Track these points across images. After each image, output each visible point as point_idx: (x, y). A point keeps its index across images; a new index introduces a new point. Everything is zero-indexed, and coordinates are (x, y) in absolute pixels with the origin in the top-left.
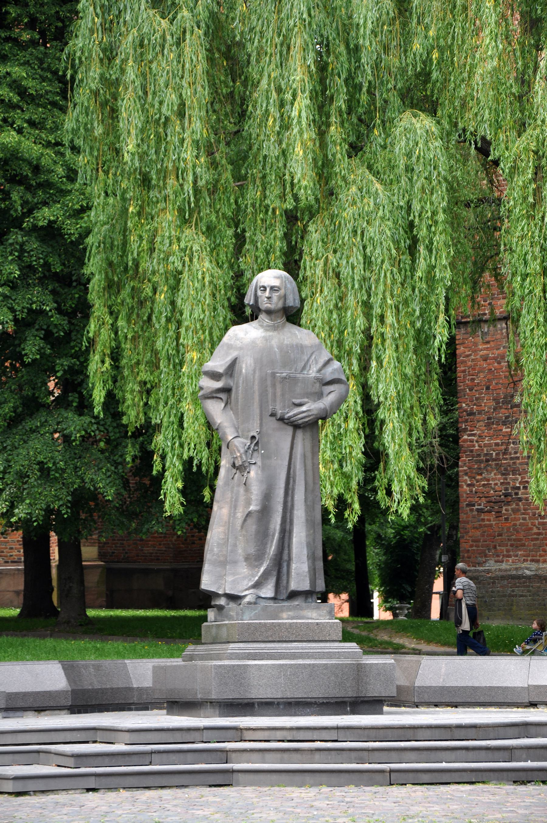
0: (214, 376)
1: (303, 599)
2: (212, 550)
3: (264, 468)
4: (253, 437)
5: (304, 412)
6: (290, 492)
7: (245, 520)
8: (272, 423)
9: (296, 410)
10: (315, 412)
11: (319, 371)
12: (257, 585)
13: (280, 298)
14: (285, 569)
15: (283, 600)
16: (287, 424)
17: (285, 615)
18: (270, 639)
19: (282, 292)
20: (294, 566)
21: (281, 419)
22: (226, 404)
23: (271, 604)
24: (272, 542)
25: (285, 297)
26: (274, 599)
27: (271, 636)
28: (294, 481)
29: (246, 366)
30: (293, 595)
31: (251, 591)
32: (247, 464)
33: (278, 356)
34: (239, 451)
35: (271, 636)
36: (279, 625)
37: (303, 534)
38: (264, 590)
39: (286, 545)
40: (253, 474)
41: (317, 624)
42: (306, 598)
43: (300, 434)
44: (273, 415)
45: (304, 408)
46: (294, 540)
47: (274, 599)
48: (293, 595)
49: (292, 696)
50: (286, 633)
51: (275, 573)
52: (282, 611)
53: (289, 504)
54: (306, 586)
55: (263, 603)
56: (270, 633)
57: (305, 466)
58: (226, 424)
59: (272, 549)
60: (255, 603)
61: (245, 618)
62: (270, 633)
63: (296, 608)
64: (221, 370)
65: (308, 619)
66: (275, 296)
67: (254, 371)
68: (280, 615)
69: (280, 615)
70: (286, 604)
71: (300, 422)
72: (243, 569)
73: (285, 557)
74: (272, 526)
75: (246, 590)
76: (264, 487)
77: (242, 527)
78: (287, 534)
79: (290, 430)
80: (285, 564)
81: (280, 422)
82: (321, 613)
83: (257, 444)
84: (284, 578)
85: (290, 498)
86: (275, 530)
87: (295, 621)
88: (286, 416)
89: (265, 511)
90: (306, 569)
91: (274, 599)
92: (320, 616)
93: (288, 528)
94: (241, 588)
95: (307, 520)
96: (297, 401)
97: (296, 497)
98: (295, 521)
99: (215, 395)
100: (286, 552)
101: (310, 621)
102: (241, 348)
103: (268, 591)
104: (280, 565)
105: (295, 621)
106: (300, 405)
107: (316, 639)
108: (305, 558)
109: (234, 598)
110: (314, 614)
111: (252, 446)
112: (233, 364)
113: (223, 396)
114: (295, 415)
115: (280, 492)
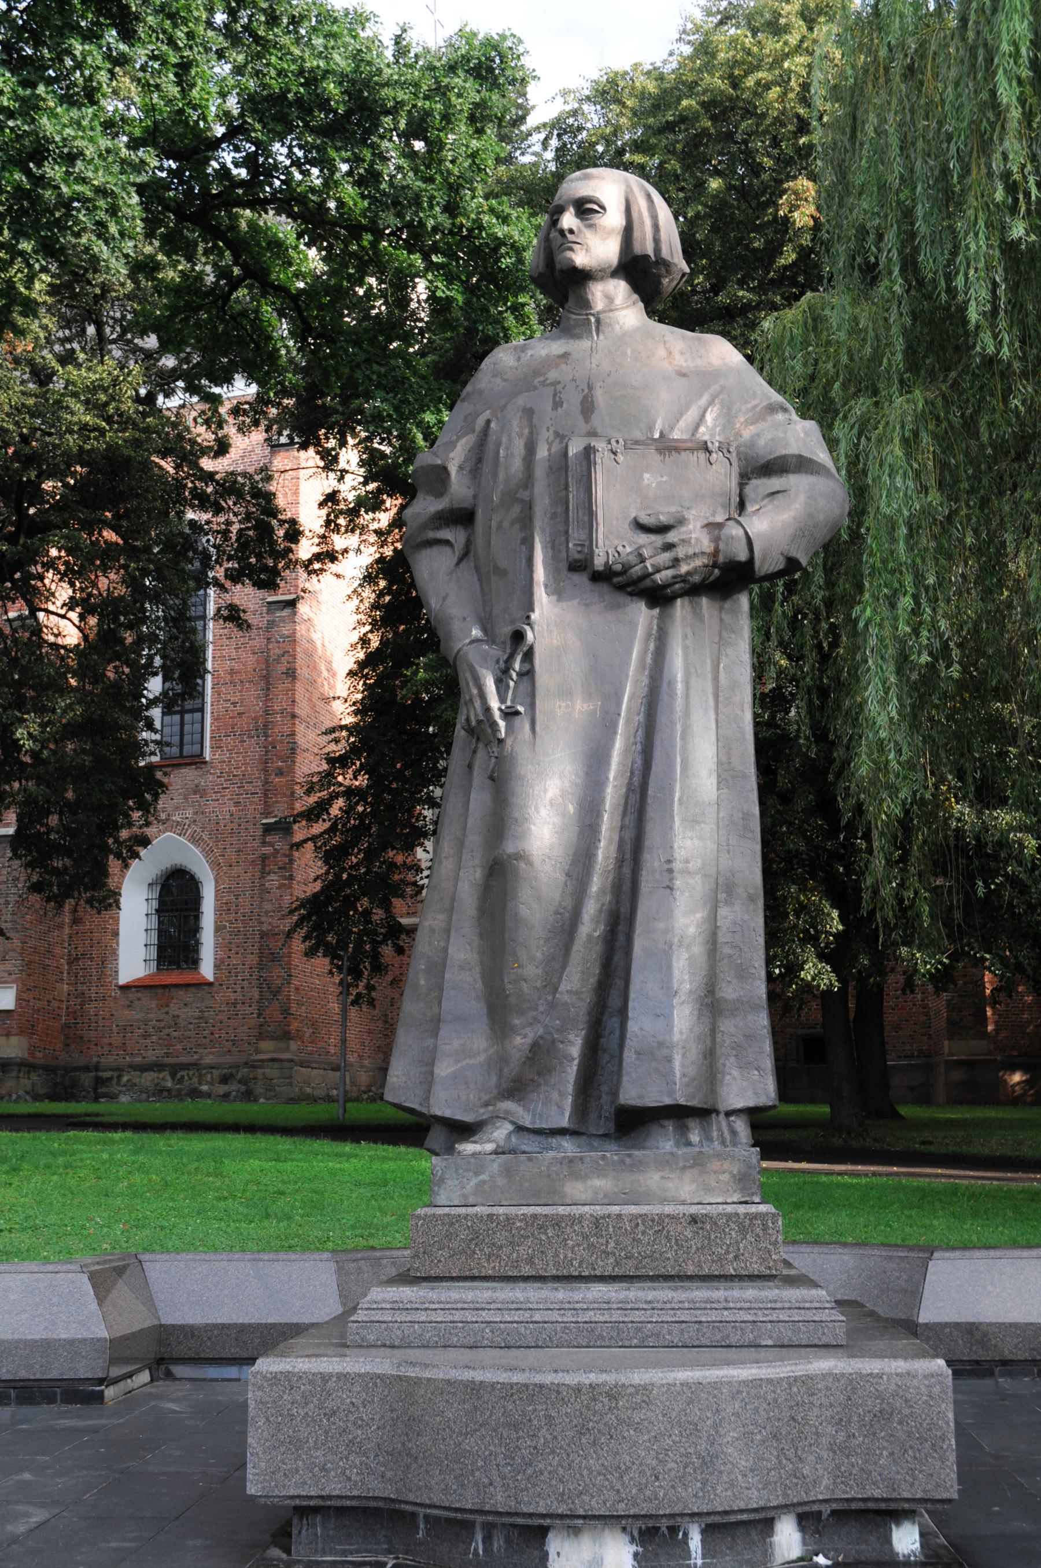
16: (621, 588)
18: (526, 1270)
20: (632, 1027)
27: (530, 1261)
35: (530, 1261)
36: (557, 1222)
41: (694, 1220)
45: (672, 537)
48: (632, 1124)
49: (512, 1505)
50: (581, 1252)
56: (523, 1251)
61: (442, 1199)
62: (523, 1251)
65: (663, 1201)
75: (487, 1104)
81: (604, 587)
87: (615, 1209)
92: (708, 1190)
99: (431, 535)
100: (619, 983)
101: (668, 1209)
105: (615, 1209)
107: (691, 1270)
113: (455, 535)
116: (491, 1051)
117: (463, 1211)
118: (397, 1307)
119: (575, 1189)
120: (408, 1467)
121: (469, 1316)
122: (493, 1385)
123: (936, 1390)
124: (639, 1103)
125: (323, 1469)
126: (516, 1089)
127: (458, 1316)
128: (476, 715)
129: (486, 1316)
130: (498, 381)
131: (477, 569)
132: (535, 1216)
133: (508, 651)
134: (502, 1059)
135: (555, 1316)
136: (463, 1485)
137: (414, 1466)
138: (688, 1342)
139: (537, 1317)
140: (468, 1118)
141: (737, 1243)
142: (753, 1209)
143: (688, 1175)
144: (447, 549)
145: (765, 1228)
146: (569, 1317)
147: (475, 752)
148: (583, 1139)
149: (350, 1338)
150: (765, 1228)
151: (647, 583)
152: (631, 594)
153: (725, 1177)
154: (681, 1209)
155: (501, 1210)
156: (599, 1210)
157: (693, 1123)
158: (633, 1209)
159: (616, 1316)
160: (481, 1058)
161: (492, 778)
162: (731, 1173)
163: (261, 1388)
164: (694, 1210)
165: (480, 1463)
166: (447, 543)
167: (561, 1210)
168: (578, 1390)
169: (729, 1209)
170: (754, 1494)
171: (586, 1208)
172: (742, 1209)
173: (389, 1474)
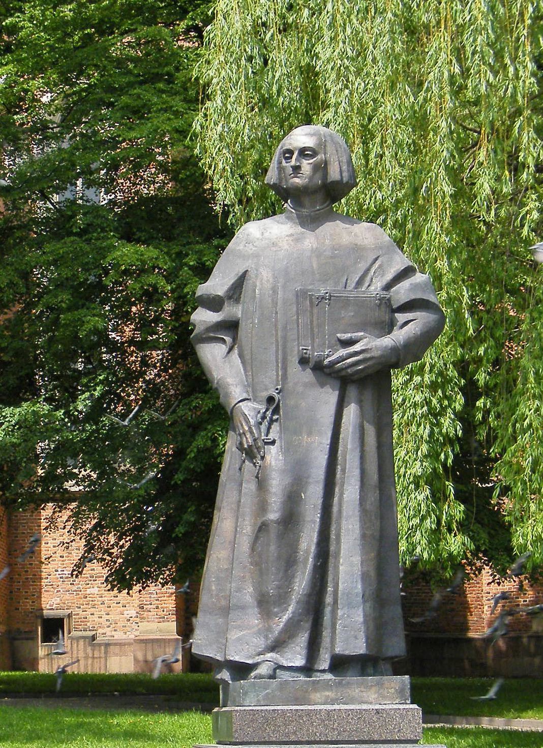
0: (215, 304)
2: (210, 590)
3: (287, 450)
4: (270, 400)
5: (356, 354)
7: (257, 538)
8: (302, 377)
9: (343, 352)
10: (376, 353)
11: (388, 287)
13: (316, 168)
14: (327, 618)
16: (329, 375)
18: (293, 738)
22: (231, 350)
24: (304, 573)
26: (308, 669)
27: (295, 733)
29: (263, 280)
30: (340, 664)
31: (269, 656)
34: (248, 422)
35: (295, 733)
37: (357, 560)
39: (330, 578)
41: (378, 712)
45: (357, 347)
50: (321, 728)
51: (307, 625)
52: (315, 690)
54: (359, 647)
55: (285, 676)
58: (230, 380)
59: (301, 584)
60: (273, 677)
61: (247, 702)
62: (291, 728)
64: (221, 292)
66: (306, 166)
67: (274, 290)
72: (254, 619)
73: (329, 599)
75: (259, 654)
76: (288, 480)
77: (253, 549)
80: (328, 610)
83: (276, 411)
84: (326, 634)
87: (336, 707)
89: (291, 519)
92: (384, 697)
101: (365, 707)
102: (256, 256)
105: (336, 707)
106: (350, 343)
107: (376, 737)
109: (242, 670)
110: (372, 695)
111: (269, 413)
112: (242, 280)
116: (261, 626)
119: (317, 696)
124: (347, 653)
126: (276, 646)
128: (247, 442)
130: (251, 246)
141: (399, 724)
142: (407, 706)
151: (343, 373)
154: (371, 707)
156: (329, 707)
160: (256, 629)
161: (257, 477)
162: (395, 688)
164: (378, 707)
167: (310, 707)
169: (395, 707)
171: (322, 707)
172: (401, 707)
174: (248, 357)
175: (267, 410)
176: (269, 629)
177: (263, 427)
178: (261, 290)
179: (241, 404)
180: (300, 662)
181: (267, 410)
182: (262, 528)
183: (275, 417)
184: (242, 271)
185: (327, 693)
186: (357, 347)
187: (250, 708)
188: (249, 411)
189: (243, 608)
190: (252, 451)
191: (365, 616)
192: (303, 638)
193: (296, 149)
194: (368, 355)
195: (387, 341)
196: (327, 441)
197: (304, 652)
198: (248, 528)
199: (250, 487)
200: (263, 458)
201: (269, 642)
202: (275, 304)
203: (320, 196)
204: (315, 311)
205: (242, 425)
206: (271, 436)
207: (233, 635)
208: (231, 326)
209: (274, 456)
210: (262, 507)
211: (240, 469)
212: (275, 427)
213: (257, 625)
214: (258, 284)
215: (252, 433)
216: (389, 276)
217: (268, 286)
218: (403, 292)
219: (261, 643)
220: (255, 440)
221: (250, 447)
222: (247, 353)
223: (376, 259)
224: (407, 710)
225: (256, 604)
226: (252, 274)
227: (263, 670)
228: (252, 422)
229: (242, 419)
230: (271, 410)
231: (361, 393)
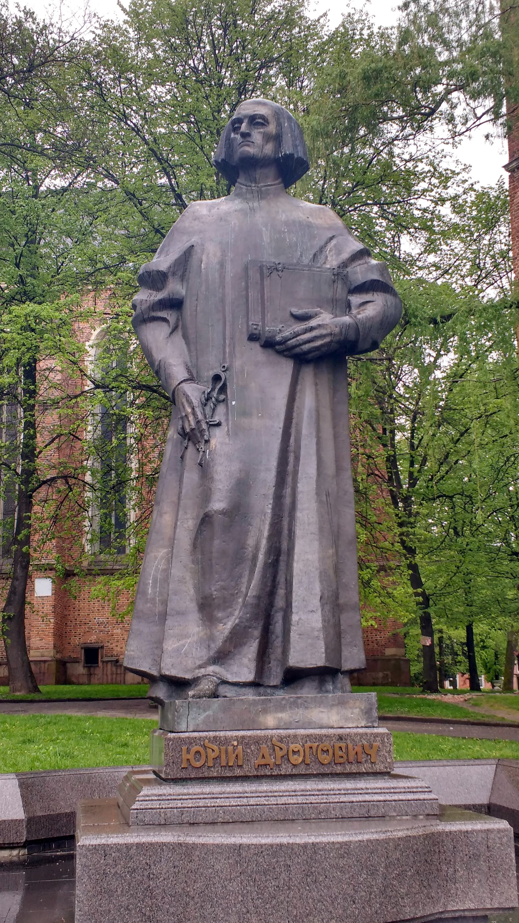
1: (315, 684)
3: (235, 433)
4: (217, 378)
5: (312, 329)
6: (289, 479)
11: (345, 265)
12: (221, 657)
14: (278, 627)
15: (275, 687)
16: (280, 353)
17: (270, 720)
18: (238, 772)
19: (272, 128)
20: (295, 618)
21: (269, 344)
22: (174, 330)
23: (250, 695)
24: (252, 572)
25: (277, 139)
28: (297, 458)
29: (209, 256)
30: (293, 677)
31: (211, 669)
32: (204, 426)
33: (266, 239)
34: (190, 403)
36: (257, 741)
38: (235, 668)
39: (281, 578)
40: (213, 442)
41: (341, 738)
42: (322, 683)
43: (308, 375)
44: (253, 338)
45: (313, 323)
46: (297, 567)
47: (255, 684)
48: (293, 677)
51: (257, 633)
52: (265, 711)
53: (287, 501)
57: (318, 430)
58: (172, 361)
59: (251, 586)
60: (215, 695)
61: (183, 727)
63: (294, 704)
67: (222, 265)
68: (261, 719)
69: (261, 719)
70: (281, 695)
71: (306, 347)
73: (280, 602)
74: (251, 542)
75: (200, 667)
76: (235, 467)
77: (194, 546)
78: (283, 558)
79: (287, 367)
81: (270, 351)
82: (348, 713)
83: (223, 389)
84: (277, 643)
85: (288, 491)
86: (257, 548)
88: (278, 338)
89: (238, 511)
90: (319, 625)
91: (255, 684)
92: (347, 719)
93: (284, 546)
94: (190, 663)
95: (321, 529)
96: (296, 311)
97: (300, 486)
98: (299, 531)
99: (154, 314)
100: (281, 592)
103: (243, 668)
104: (269, 616)
105: (291, 732)
108: (316, 602)
111: (215, 394)
113: (170, 315)
114: (297, 335)
115: (269, 476)
116: (202, 634)
117: (196, 734)
118: (160, 798)
120: (187, 904)
121: (209, 803)
122: (249, 846)
123: (505, 840)
124: (302, 665)
125: (127, 909)
126: (221, 657)
127: (201, 803)
128: (190, 425)
129: (219, 802)
130: (197, 222)
131: (185, 337)
132: (243, 737)
133: (211, 387)
134: (211, 638)
135: (263, 801)
136: (228, 914)
137: (192, 903)
138: (344, 814)
139: (252, 801)
140: (188, 676)
142: (375, 730)
143: (334, 711)
144: (164, 324)
145: (383, 742)
146: (273, 801)
147: (186, 448)
148: (261, 690)
149: (132, 820)
150: (383, 742)
151: (298, 350)
152: (286, 356)
153: (357, 711)
154: (331, 731)
155: (222, 734)
157: (329, 678)
158: (302, 732)
159: (300, 800)
160: (195, 638)
161: (200, 464)
162: (360, 708)
163: (86, 856)
165: (240, 898)
166: (164, 320)
168: (305, 846)
169: (361, 731)
170: (407, 910)
171: (274, 731)
173: (172, 910)
174: (192, 336)
175: (213, 390)
176: (211, 638)
177: (208, 409)
178: (207, 264)
179: (184, 385)
180: (249, 676)
181: (213, 390)
182: (206, 520)
183: (222, 397)
184: (188, 244)
185: (280, 715)
186: (313, 323)
187: (187, 734)
188: (193, 392)
189: (181, 613)
190: (195, 435)
191: (324, 621)
192: (251, 649)
193: (245, 116)
194: (324, 332)
195: (346, 319)
196: (279, 425)
197: (253, 665)
198: (188, 523)
199: (191, 476)
200: (207, 442)
201: (212, 653)
202: (222, 277)
203: (271, 172)
204: (267, 282)
205: (184, 407)
206: (217, 419)
207: (169, 645)
208: (175, 304)
209: (218, 439)
210: (206, 496)
211: (182, 457)
212: (221, 409)
213: (198, 633)
214: (204, 258)
215: (194, 413)
216: (345, 256)
217: (215, 261)
218: (360, 273)
219: (203, 654)
220: (198, 422)
221: (192, 430)
222: (191, 332)
223: (331, 238)
224: (376, 735)
225: (196, 608)
226: (197, 249)
227: (205, 686)
228: (196, 402)
229: (184, 400)
230: (216, 390)
231: (315, 375)
